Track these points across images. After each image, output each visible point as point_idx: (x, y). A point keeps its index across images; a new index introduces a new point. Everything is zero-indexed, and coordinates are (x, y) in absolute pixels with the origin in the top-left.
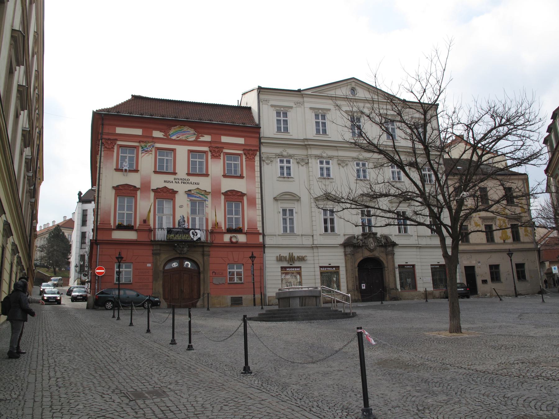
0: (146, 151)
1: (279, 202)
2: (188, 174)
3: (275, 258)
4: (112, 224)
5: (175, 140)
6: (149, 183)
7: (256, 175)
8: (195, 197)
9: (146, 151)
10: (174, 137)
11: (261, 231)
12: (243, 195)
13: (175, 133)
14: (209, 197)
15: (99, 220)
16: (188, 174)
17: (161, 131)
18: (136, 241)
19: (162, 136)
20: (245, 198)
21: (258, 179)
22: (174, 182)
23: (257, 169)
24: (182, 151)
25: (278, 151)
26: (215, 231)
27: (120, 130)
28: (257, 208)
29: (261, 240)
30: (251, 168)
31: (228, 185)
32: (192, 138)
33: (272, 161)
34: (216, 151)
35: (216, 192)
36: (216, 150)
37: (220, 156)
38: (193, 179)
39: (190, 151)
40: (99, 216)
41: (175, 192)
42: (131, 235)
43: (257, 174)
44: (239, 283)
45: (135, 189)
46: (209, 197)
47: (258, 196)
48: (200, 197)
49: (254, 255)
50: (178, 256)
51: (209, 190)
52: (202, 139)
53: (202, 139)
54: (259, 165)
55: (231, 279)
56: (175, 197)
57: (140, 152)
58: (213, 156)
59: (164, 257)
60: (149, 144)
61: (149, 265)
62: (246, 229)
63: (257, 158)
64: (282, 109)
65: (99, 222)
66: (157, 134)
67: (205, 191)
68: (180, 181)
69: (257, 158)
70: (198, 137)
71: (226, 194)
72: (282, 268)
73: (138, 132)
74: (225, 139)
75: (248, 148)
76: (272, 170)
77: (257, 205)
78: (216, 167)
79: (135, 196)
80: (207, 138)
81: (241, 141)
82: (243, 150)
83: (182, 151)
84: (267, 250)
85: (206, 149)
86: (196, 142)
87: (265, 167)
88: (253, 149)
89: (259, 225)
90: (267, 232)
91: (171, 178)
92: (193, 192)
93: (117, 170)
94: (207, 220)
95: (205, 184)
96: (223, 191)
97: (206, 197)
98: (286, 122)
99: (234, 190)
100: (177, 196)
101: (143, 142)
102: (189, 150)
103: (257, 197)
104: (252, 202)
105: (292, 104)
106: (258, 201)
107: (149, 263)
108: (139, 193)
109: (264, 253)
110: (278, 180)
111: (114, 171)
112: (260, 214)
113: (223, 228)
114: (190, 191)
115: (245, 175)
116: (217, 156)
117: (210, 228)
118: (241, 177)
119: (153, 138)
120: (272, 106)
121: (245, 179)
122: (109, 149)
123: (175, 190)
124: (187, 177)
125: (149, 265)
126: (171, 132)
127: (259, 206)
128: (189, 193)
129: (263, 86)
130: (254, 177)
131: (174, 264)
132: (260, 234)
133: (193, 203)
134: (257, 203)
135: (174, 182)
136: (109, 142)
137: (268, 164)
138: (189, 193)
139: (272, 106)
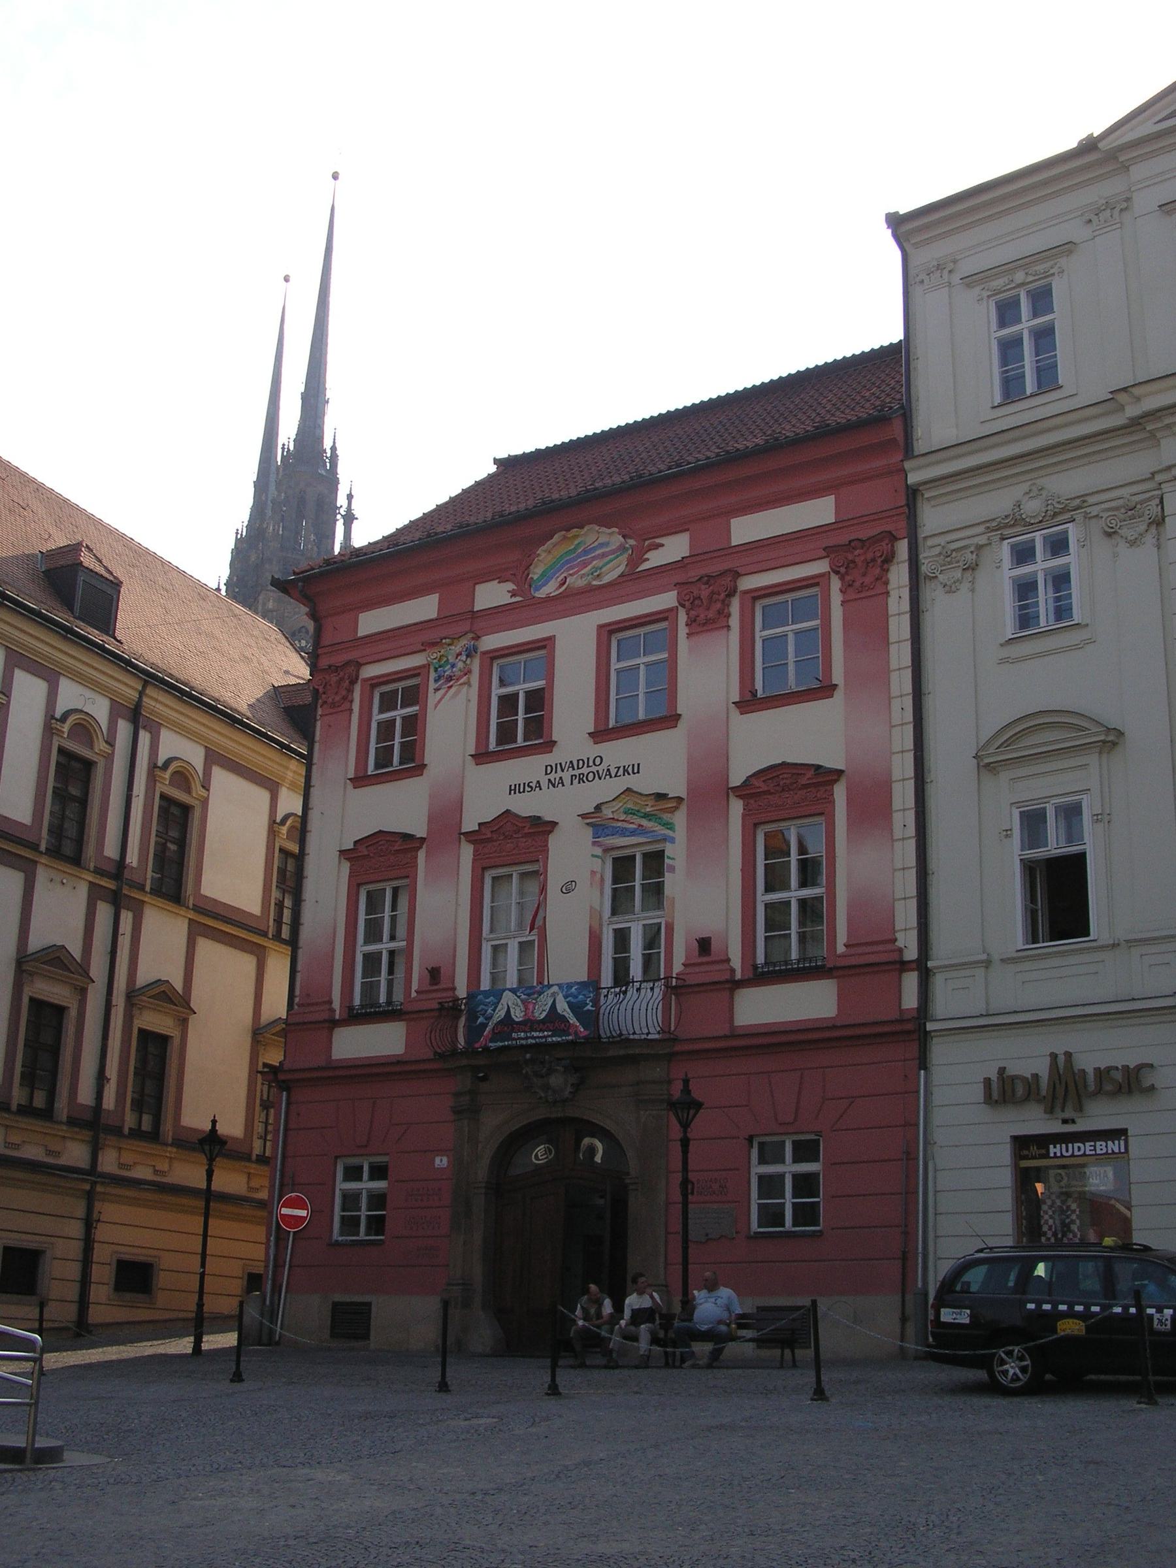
0: (450, 678)
1: (1005, 776)
2: (601, 734)
3: (978, 1092)
4: (336, 1005)
5: (549, 599)
6: (458, 807)
7: (894, 664)
8: (623, 833)
9: (450, 678)
10: (550, 589)
11: (912, 954)
12: (825, 777)
13: (550, 569)
14: (680, 819)
15: (297, 992)
16: (601, 734)
17: (502, 580)
18: (397, 1061)
19: (507, 599)
20: (840, 792)
21: (902, 682)
22: (544, 784)
23: (900, 627)
24: (575, 638)
25: (997, 502)
26: (707, 979)
27: (371, 622)
28: (898, 833)
29: (910, 1000)
30: (869, 631)
31: (766, 741)
32: (614, 570)
33: (972, 568)
34: (708, 594)
35: (708, 792)
36: (705, 592)
37: (725, 614)
38: (616, 752)
39: (607, 631)
40: (299, 977)
41: (541, 828)
42: (383, 1041)
43: (900, 655)
44: (803, 1235)
45: (408, 843)
46: (680, 819)
47: (903, 767)
48: (640, 831)
49: (696, 1094)
50: (541, 1113)
51: (677, 787)
52: (655, 559)
53: (655, 559)
54: (906, 606)
55: (773, 1216)
56: (545, 849)
57: (432, 685)
58: (698, 626)
59: (494, 1123)
60: (457, 648)
61: (441, 1162)
62: (841, 949)
63: (899, 575)
64: (1020, 277)
65: (297, 1000)
66: (492, 594)
67: (661, 797)
68: (566, 776)
69: (899, 575)
70: (637, 557)
71: (746, 791)
72: (1021, 1144)
73: (425, 608)
74: (747, 529)
75: (844, 539)
76: (969, 617)
77: (897, 818)
78: (707, 673)
79: (410, 874)
80: (675, 548)
81: (819, 512)
82: (829, 551)
83: (575, 638)
84: (939, 1051)
85: (667, 600)
86: (635, 581)
87: (942, 609)
88: (863, 534)
89: (906, 916)
90: (943, 949)
91: (530, 768)
92: (607, 812)
93: (361, 780)
94: (670, 928)
95: (661, 762)
96: (736, 780)
97: (669, 826)
98: (1044, 337)
99: (784, 765)
100: (553, 841)
101: (433, 644)
102: (600, 627)
103: (896, 774)
104: (872, 808)
105: (1074, 231)
106: (903, 796)
107: (441, 1152)
108: (421, 855)
109: (923, 1063)
110: (1003, 661)
111: (350, 785)
112: (912, 861)
113: (736, 962)
114: (598, 808)
115: (838, 677)
116: (714, 621)
117: (677, 968)
118: (826, 690)
119: (474, 615)
120: (970, 281)
121: (839, 695)
122: (333, 705)
123: (548, 818)
124: (591, 750)
125: (441, 1162)
126: (536, 572)
127: (904, 820)
128: (596, 821)
129: (905, 207)
130: (883, 674)
131: (540, 1150)
132: (903, 966)
133: (622, 867)
134: (897, 804)
135: (544, 784)
136: (334, 678)
137: (950, 589)
138: (596, 821)
139: (970, 281)
